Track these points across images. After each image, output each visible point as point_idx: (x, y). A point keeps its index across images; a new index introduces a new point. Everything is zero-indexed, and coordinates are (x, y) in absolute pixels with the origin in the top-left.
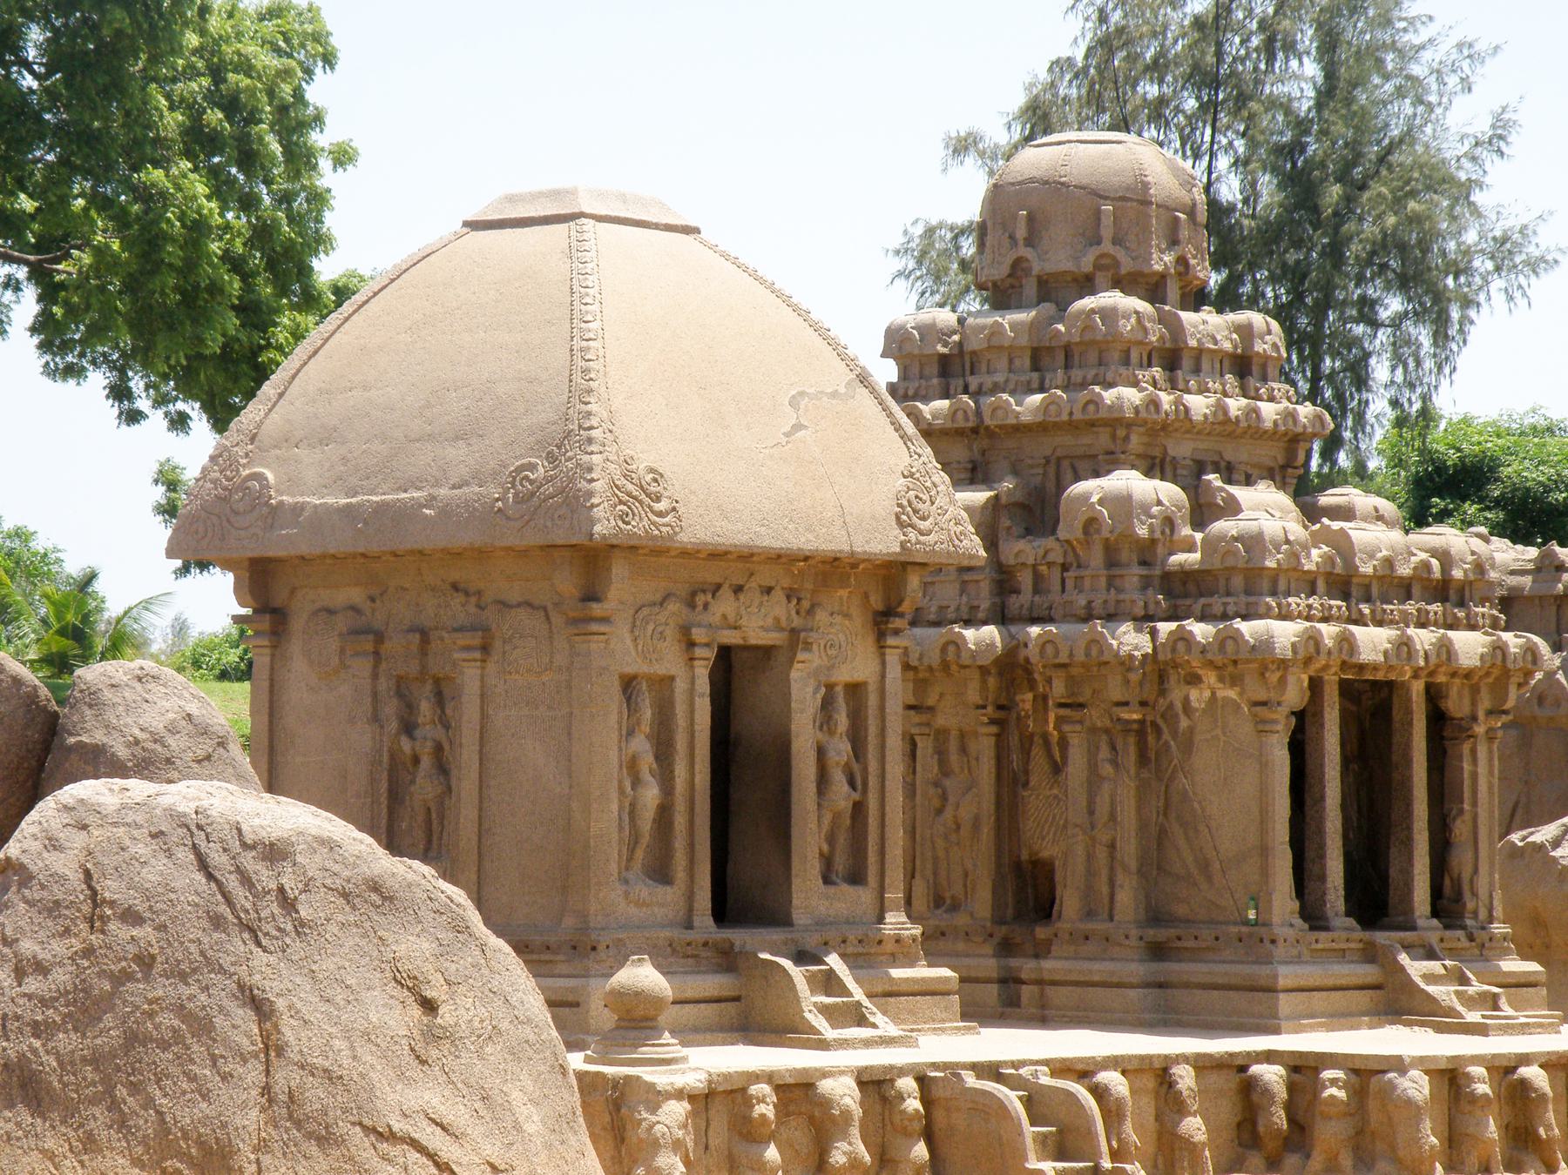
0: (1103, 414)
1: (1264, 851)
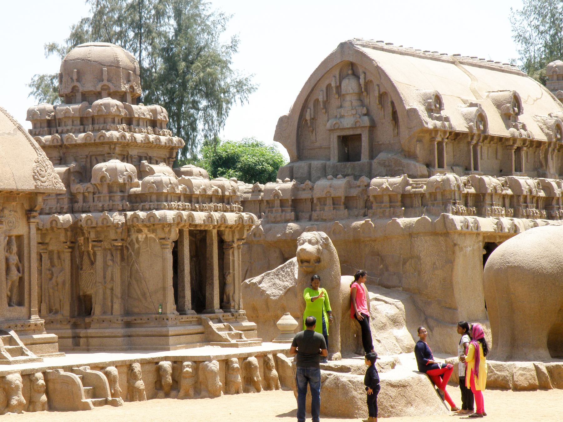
0: (106, 140)
1: (164, 289)
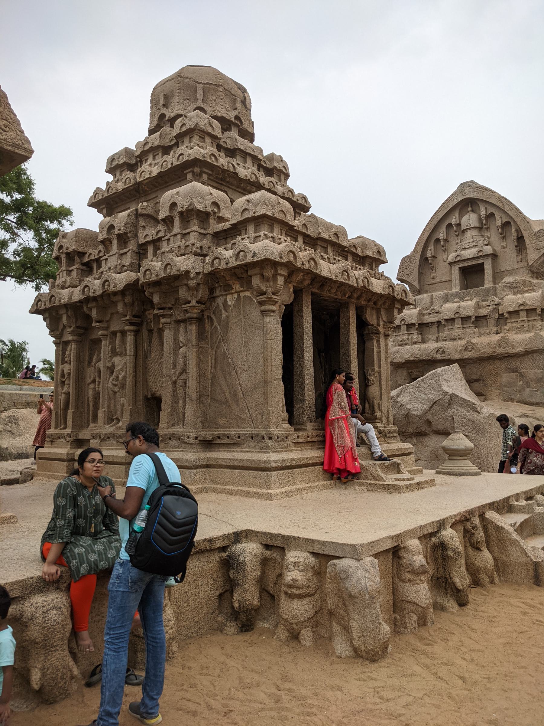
1: (265, 383)
